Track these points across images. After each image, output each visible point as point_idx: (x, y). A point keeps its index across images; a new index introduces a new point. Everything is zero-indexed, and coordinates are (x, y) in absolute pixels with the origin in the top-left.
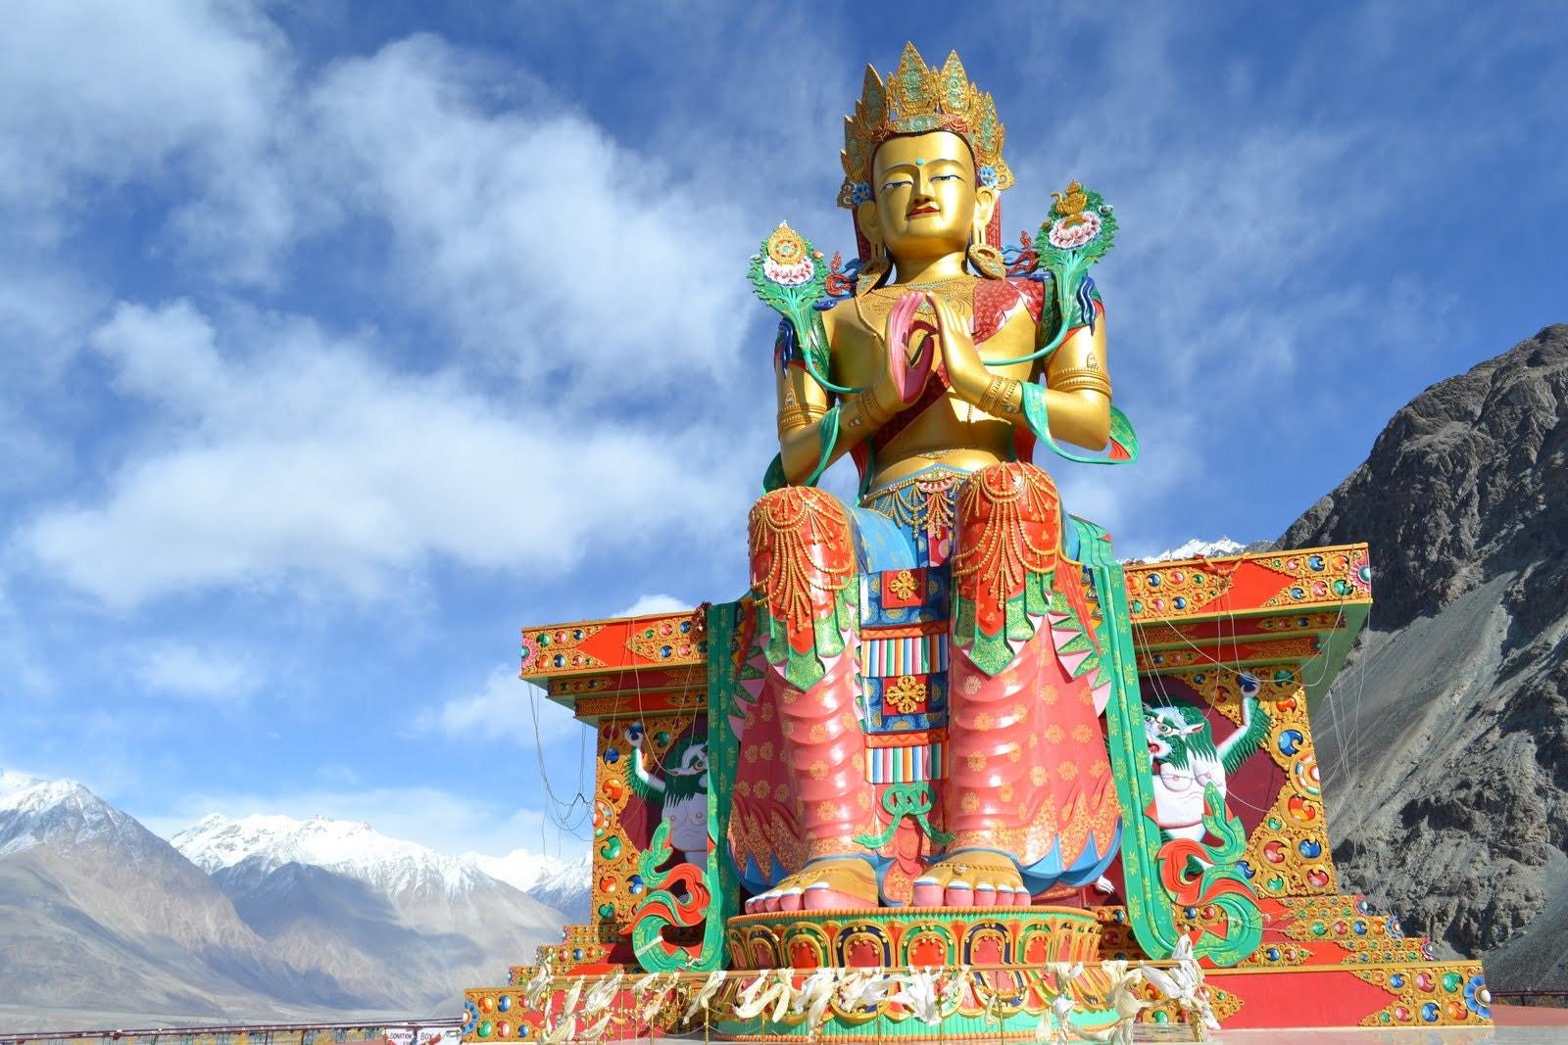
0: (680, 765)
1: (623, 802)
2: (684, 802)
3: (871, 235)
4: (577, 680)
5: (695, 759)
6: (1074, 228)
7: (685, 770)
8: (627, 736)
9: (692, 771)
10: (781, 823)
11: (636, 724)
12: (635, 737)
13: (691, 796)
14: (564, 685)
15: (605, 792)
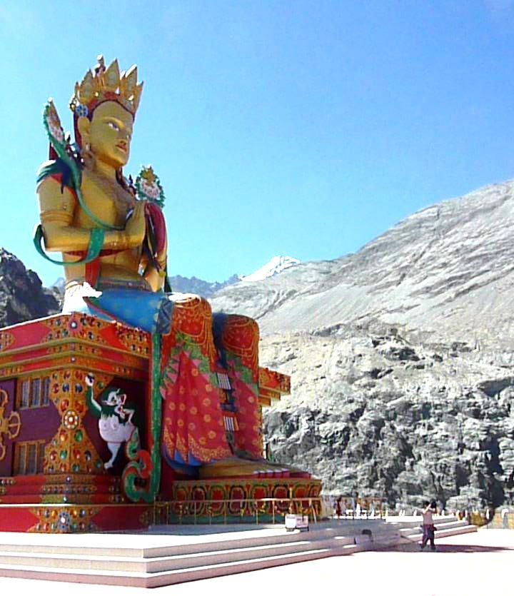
0: (107, 400)
1: (83, 414)
2: (109, 418)
3: (84, 134)
4: (88, 346)
5: (113, 398)
6: (150, 188)
7: (109, 403)
8: (87, 380)
9: (112, 404)
10: (192, 439)
11: (91, 374)
12: (91, 381)
13: (111, 416)
14: (93, 350)
15: (76, 406)
